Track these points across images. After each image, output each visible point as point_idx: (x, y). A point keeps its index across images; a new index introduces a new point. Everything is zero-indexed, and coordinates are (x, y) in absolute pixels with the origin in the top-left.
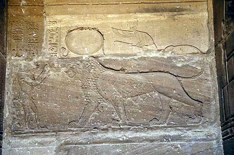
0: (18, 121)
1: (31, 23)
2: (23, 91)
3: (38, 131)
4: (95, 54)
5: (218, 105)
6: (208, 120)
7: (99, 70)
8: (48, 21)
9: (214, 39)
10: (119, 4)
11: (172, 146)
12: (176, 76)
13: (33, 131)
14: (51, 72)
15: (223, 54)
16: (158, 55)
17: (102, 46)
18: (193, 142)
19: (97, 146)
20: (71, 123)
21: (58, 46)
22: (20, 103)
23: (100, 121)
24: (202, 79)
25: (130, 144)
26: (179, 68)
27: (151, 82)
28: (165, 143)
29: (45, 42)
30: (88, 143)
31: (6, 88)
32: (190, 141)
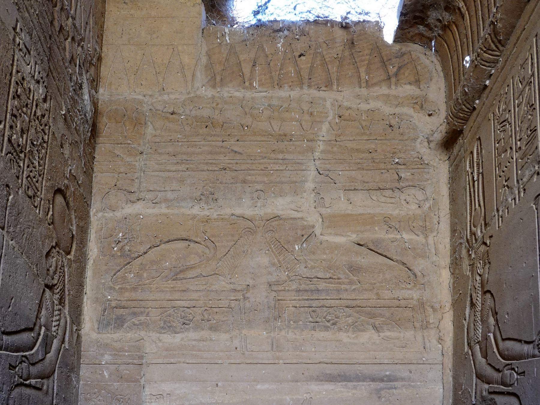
1: (119, 396)
10: (279, 364)
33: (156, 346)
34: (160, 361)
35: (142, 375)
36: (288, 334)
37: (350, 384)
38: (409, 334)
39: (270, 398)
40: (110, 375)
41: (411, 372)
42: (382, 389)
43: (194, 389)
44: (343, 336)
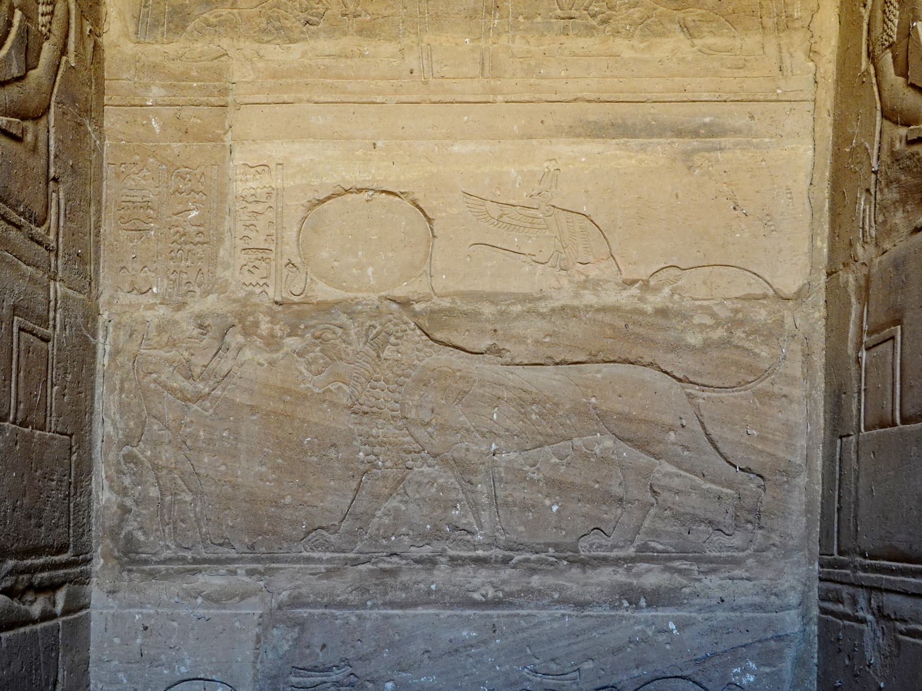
0: (139, 519)
2: (155, 417)
3: (205, 555)
4: (400, 292)
5: (819, 488)
6: (776, 539)
7: (412, 349)
8: (241, 162)
9: (825, 245)
10: (494, 102)
11: (648, 626)
12: (680, 380)
13: (189, 555)
14: (248, 354)
15: (853, 316)
16: (625, 298)
17: (428, 260)
18: (721, 614)
19: (397, 615)
20: (314, 534)
21: (272, 256)
22: (146, 457)
23: (411, 533)
24: (770, 396)
25: (506, 612)
26: (692, 349)
27: (593, 400)
28: (626, 613)
29: (227, 244)
30: (369, 603)
31: (98, 406)
32: (710, 609)
33: (253, 69)
34: (262, 98)
35: (227, 126)
36: (513, 41)
37: (633, 142)
38: (752, 41)
39: (479, 171)
40: (164, 127)
41: (752, 117)
42: (695, 151)
43: (329, 153)
44: (621, 46)
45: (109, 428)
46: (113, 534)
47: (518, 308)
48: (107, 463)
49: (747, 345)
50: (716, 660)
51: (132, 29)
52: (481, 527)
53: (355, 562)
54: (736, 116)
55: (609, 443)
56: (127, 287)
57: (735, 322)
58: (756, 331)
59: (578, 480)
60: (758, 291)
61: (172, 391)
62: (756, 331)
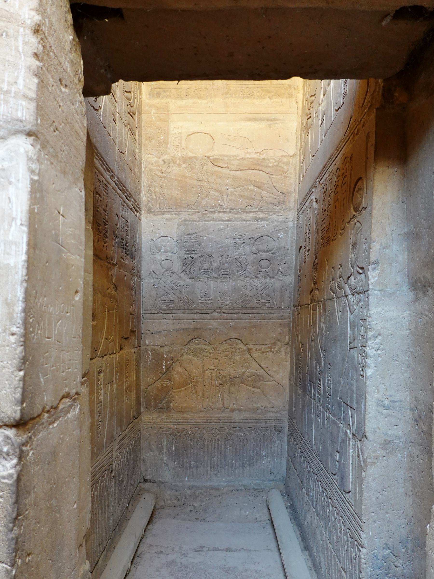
4: (207, 155)
5: (297, 196)
6: (288, 207)
7: (210, 167)
13: (162, 210)
14: (174, 168)
16: (256, 156)
18: (276, 223)
24: (287, 177)
26: (270, 167)
31: (142, 179)
32: (274, 222)
34: (177, 112)
37: (258, 122)
38: (284, 100)
42: (271, 124)
44: (255, 101)
45: (145, 184)
46: (146, 206)
47: (232, 158)
48: (144, 191)
49: (282, 166)
50: (275, 232)
51: (148, 97)
52: (225, 205)
53: (198, 212)
54: (280, 117)
55: (252, 187)
56: (148, 153)
57: (279, 161)
58: (284, 163)
59: (245, 195)
60: (284, 154)
61: (158, 176)
62: (284, 163)
